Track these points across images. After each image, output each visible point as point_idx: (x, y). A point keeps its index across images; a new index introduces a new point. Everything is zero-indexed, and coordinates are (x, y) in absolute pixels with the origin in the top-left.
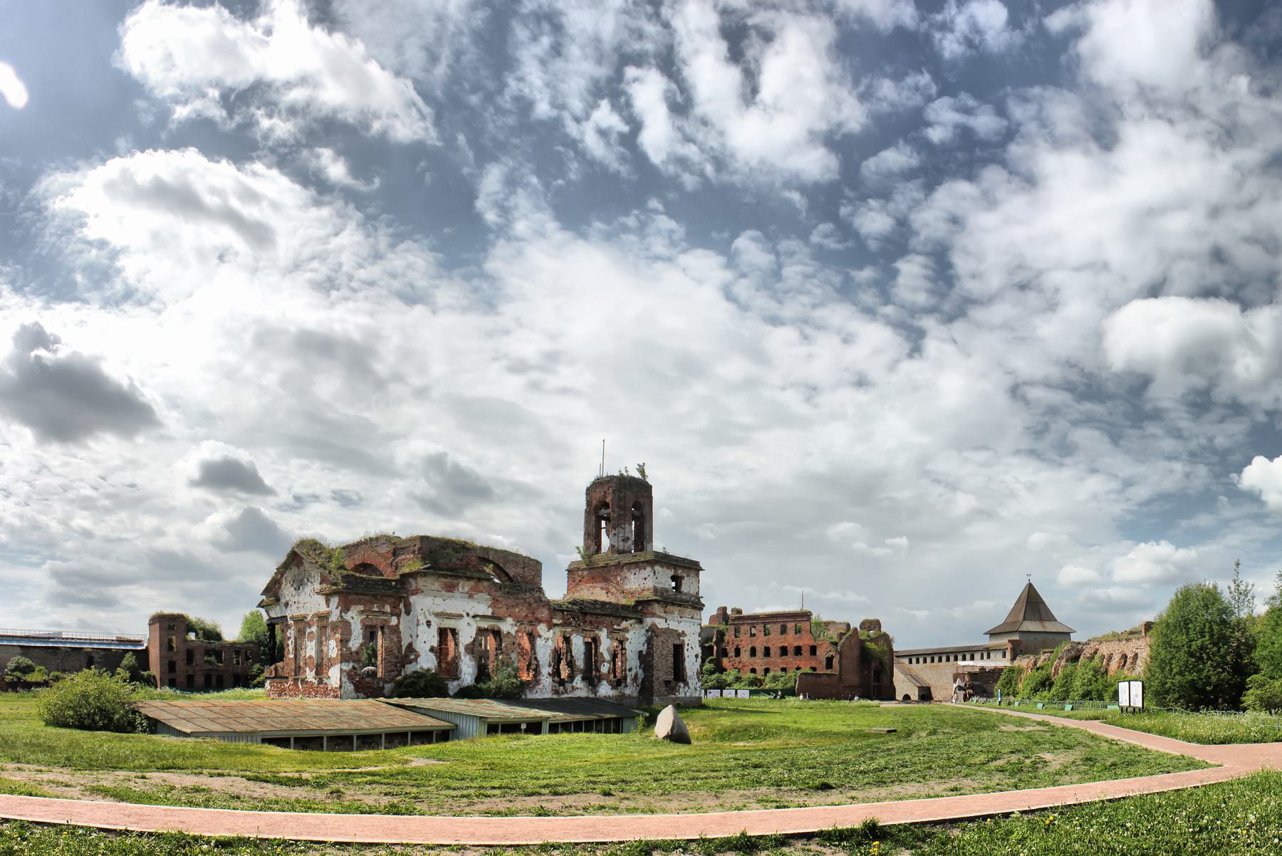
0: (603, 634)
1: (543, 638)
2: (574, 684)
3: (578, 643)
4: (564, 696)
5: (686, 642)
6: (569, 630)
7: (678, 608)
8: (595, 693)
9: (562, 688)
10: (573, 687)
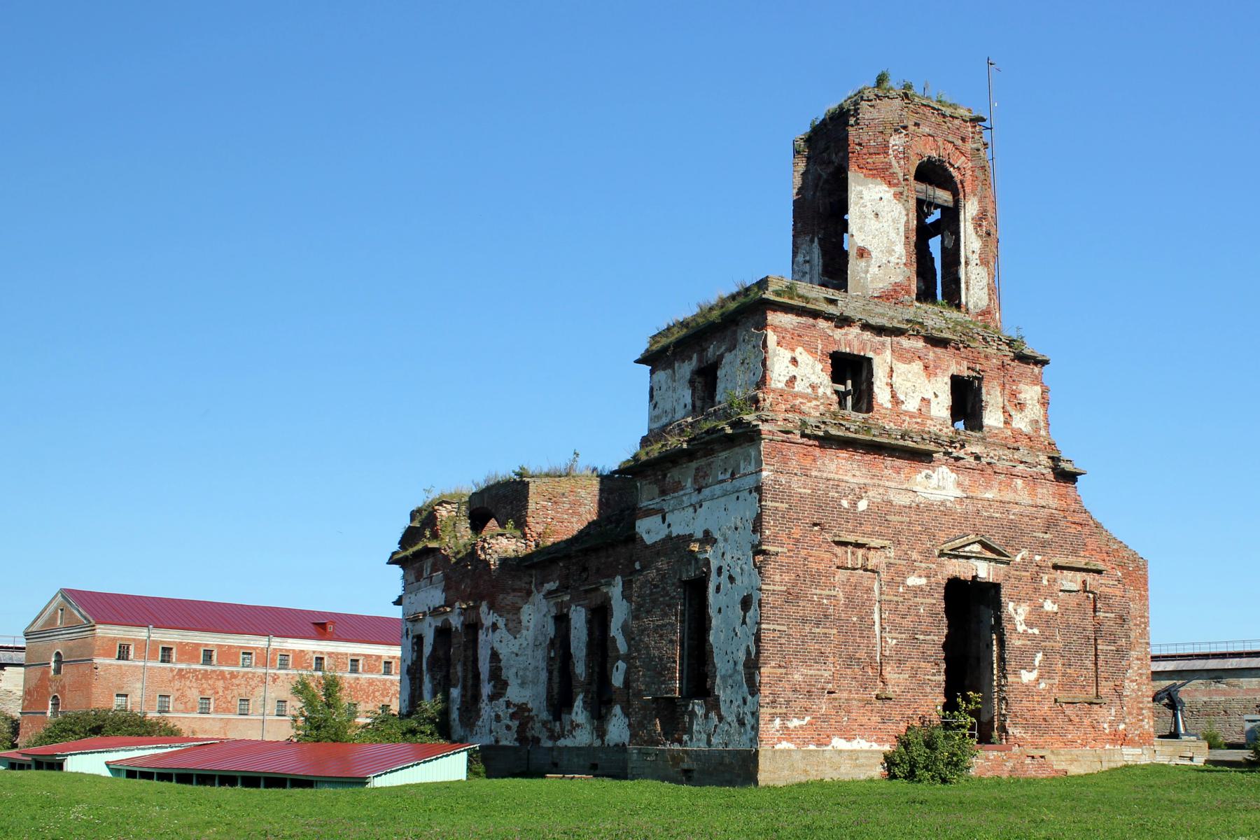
0: (616, 590)
1: (484, 629)
2: (573, 716)
3: (578, 618)
4: (562, 743)
5: (714, 565)
6: (567, 598)
7: (694, 465)
8: (601, 733)
9: (558, 724)
10: (572, 722)
